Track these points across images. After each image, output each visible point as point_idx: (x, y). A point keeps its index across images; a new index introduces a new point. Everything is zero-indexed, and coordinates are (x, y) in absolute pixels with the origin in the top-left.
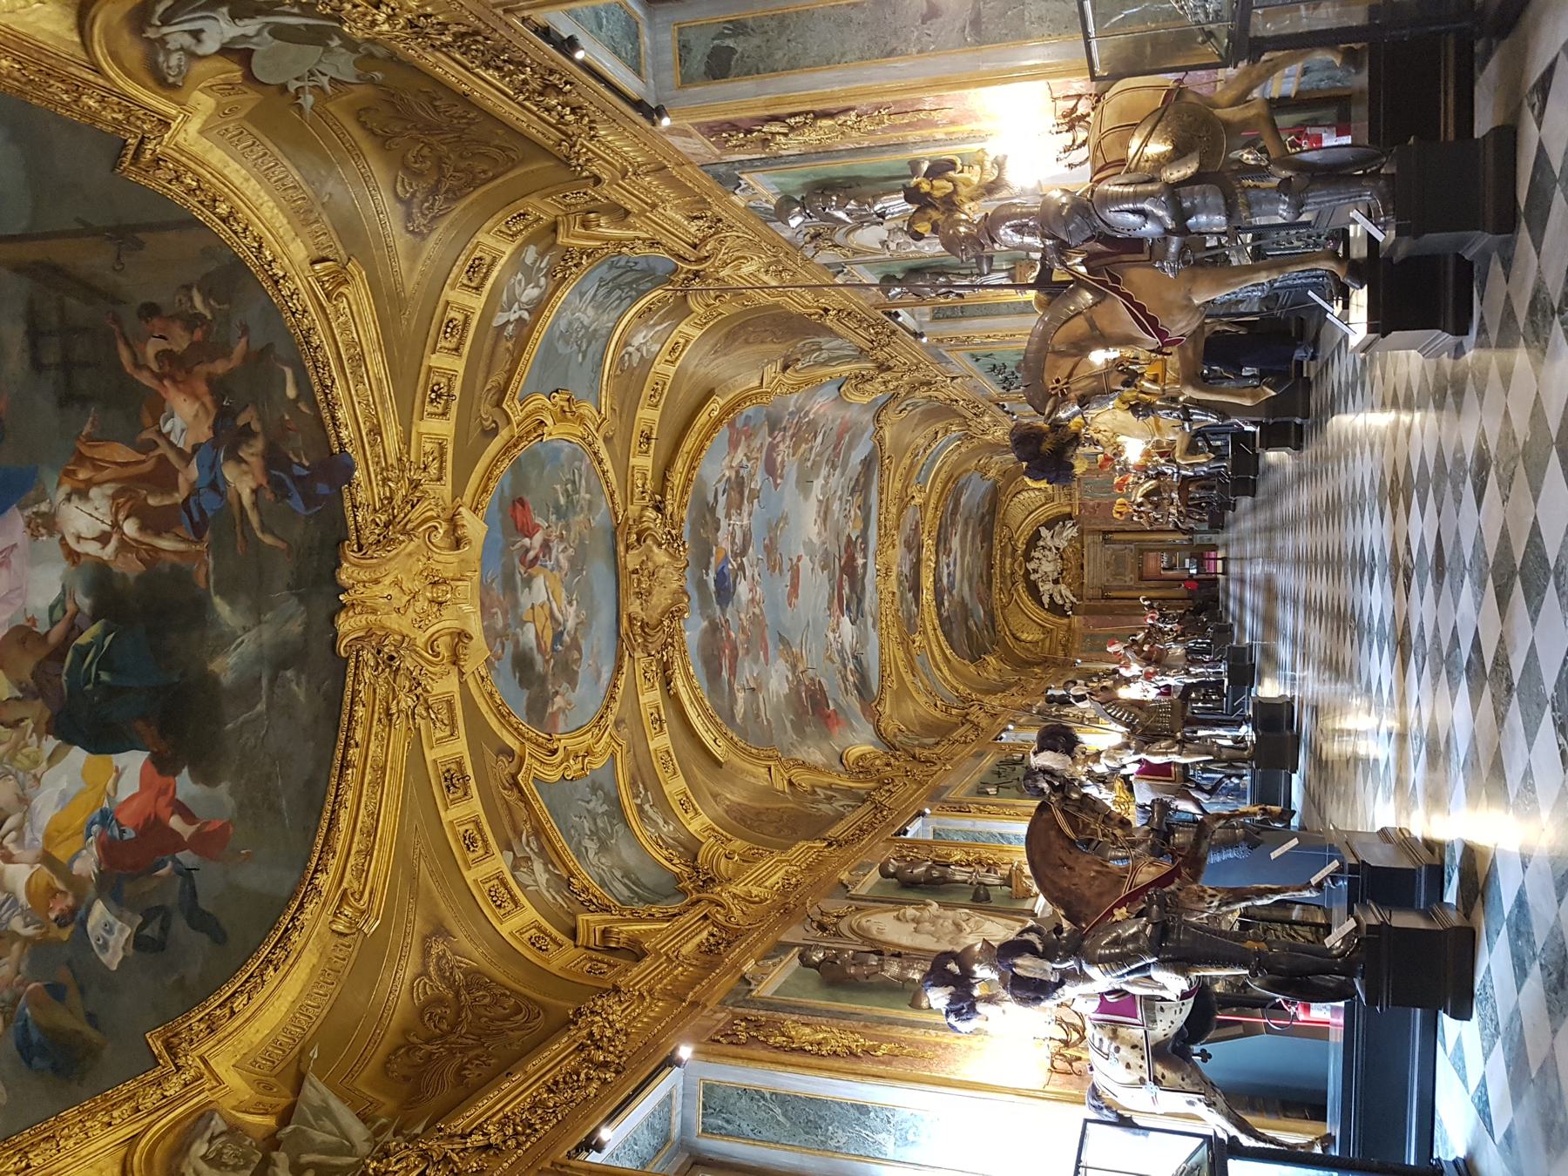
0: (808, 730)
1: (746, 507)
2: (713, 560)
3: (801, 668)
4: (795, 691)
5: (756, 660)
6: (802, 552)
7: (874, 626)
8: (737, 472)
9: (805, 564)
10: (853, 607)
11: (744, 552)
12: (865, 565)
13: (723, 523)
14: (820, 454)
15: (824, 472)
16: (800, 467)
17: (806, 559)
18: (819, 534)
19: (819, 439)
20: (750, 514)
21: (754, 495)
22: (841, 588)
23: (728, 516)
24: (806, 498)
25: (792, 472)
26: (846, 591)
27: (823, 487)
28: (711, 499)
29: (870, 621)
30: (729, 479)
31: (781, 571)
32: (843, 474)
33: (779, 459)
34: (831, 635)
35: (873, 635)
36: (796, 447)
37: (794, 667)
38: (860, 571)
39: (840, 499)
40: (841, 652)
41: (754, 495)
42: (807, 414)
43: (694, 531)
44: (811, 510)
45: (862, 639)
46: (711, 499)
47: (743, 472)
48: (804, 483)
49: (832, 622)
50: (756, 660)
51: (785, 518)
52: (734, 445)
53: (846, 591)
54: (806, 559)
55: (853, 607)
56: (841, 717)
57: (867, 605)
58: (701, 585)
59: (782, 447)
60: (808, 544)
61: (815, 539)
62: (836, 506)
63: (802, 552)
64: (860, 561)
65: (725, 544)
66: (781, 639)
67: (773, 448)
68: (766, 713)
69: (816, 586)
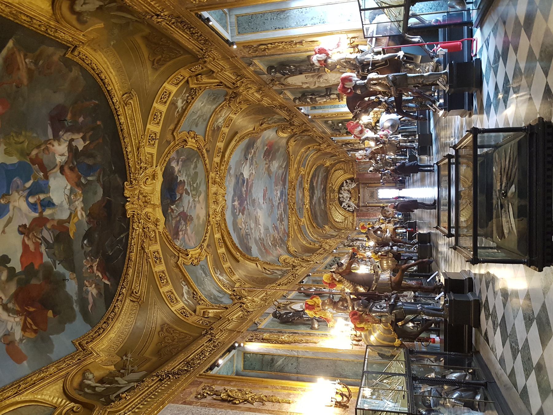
0: (277, 147)
3: (267, 165)
4: (271, 161)
5: (279, 174)
6: (263, 205)
7: (230, 168)
9: (261, 201)
10: (241, 181)
11: (279, 203)
12: (233, 201)
14: (267, 240)
15: (262, 235)
17: (261, 203)
18: (257, 213)
22: (246, 191)
24: (264, 225)
25: (271, 230)
26: (244, 189)
27: (260, 230)
29: (232, 172)
31: (269, 199)
32: (255, 239)
34: (254, 172)
35: (232, 162)
36: (274, 237)
37: (269, 167)
38: (236, 198)
39: (251, 229)
40: (251, 164)
41: (278, 220)
44: (262, 221)
45: (239, 164)
48: (267, 229)
49: (252, 177)
50: (279, 174)
51: (269, 216)
53: (244, 189)
54: (261, 203)
55: (241, 181)
56: (267, 143)
57: (233, 180)
58: (285, 196)
60: (261, 209)
61: (258, 210)
62: (253, 225)
63: (263, 205)
64: (236, 203)
65: (282, 205)
66: (270, 177)
67: (279, 234)
68: (282, 159)
69: (258, 193)
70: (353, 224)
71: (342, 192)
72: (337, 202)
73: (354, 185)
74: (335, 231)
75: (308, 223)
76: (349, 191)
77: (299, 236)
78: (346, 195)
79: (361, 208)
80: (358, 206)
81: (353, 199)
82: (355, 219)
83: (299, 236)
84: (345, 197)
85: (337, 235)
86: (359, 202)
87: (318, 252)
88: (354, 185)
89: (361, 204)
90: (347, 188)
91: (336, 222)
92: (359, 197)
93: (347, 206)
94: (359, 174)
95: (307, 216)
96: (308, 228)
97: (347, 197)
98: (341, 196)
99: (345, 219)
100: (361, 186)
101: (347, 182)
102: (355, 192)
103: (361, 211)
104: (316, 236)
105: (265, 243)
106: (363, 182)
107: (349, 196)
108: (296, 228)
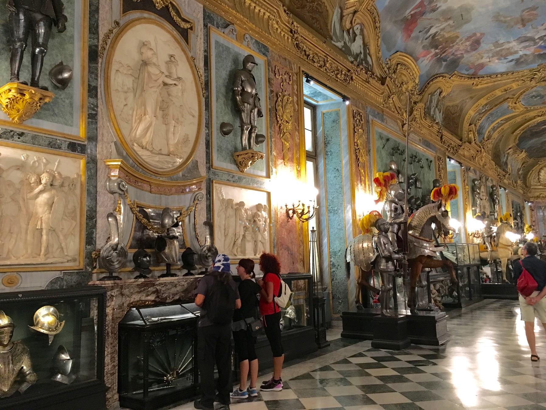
1: (507, 46)
2: (542, 53)
8: (493, 57)
11: (532, 39)
13: (521, 53)
16: (459, 26)
19: (433, 31)
20: (509, 42)
21: (496, 44)
23: (516, 52)
25: (468, 28)
28: (513, 63)
30: (498, 59)
33: (468, 43)
36: (452, 40)
41: (496, 44)
42: (436, 54)
43: (532, 63)
46: (513, 63)
47: (491, 55)
52: (482, 66)
59: (462, 48)
70: (538, 197)
74: (519, 170)
75: (519, 119)
77: (483, 101)
83: (483, 101)
85: (507, 172)
87: (445, 133)
91: (539, 172)
95: (532, 114)
96: (507, 120)
104: (495, 135)
105: (429, 16)
108: (498, 93)
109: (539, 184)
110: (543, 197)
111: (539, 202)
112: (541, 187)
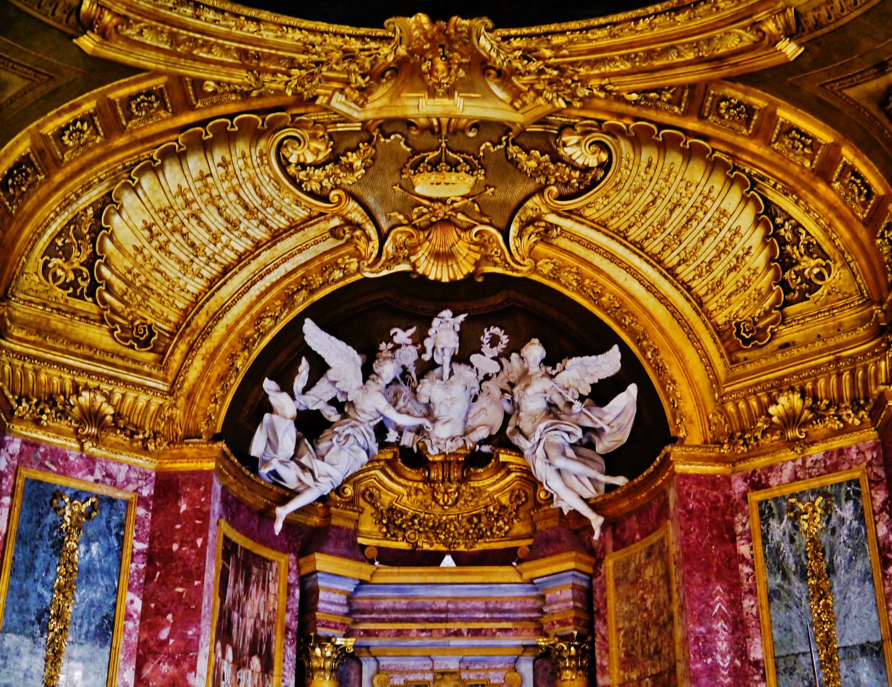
71: (484, 362)
72: (367, 264)
73: (571, 487)
76: (501, 440)
78: (454, 410)
79: (282, 564)
80: (305, 538)
81: (399, 491)
82: (130, 468)
84: (429, 389)
86: (358, 553)
88: (571, 487)
89: (336, 575)
90: (532, 401)
92: (434, 559)
93: (317, 399)
94: (716, 515)
97: (429, 412)
98: (445, 332)
99: (142, 337)
100: (560, 570)
101: (602, 393)
102: (479, 525)
103: (243, 566)
106: (614, 604)
107: (444, 438)
109: (87, 306)
110: (92, 416)
111: (56, 455)
112: (99, 335)
